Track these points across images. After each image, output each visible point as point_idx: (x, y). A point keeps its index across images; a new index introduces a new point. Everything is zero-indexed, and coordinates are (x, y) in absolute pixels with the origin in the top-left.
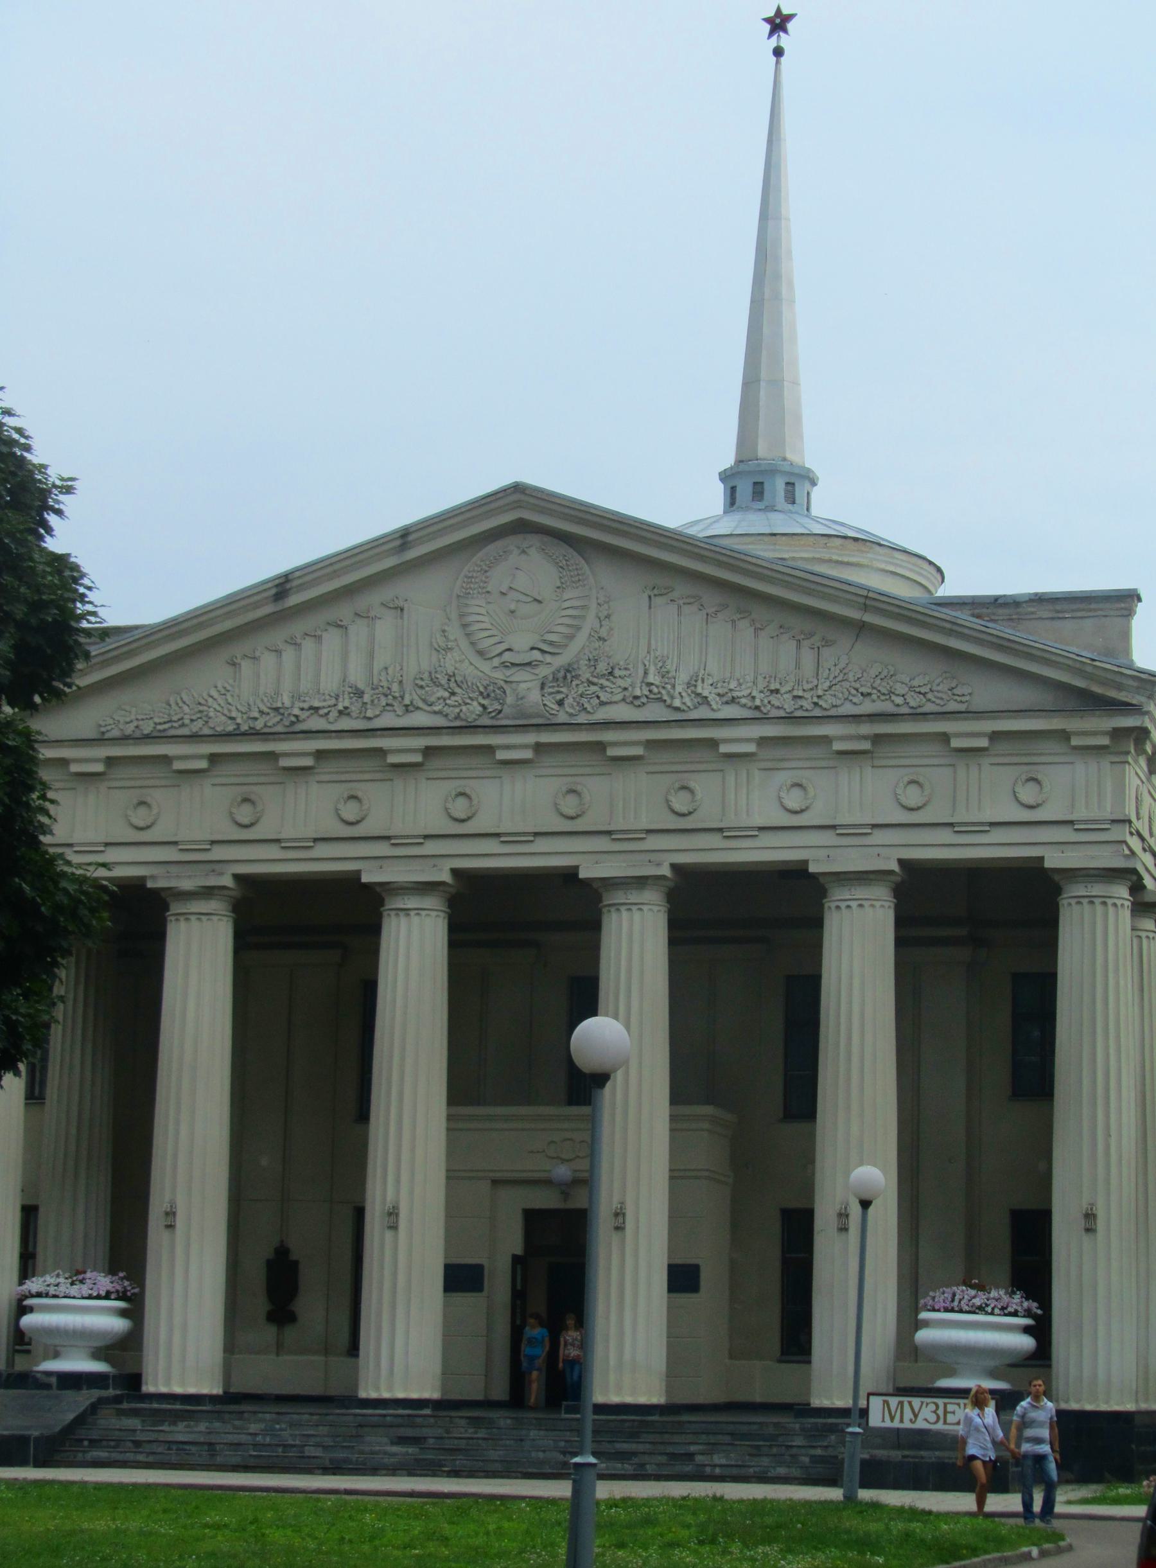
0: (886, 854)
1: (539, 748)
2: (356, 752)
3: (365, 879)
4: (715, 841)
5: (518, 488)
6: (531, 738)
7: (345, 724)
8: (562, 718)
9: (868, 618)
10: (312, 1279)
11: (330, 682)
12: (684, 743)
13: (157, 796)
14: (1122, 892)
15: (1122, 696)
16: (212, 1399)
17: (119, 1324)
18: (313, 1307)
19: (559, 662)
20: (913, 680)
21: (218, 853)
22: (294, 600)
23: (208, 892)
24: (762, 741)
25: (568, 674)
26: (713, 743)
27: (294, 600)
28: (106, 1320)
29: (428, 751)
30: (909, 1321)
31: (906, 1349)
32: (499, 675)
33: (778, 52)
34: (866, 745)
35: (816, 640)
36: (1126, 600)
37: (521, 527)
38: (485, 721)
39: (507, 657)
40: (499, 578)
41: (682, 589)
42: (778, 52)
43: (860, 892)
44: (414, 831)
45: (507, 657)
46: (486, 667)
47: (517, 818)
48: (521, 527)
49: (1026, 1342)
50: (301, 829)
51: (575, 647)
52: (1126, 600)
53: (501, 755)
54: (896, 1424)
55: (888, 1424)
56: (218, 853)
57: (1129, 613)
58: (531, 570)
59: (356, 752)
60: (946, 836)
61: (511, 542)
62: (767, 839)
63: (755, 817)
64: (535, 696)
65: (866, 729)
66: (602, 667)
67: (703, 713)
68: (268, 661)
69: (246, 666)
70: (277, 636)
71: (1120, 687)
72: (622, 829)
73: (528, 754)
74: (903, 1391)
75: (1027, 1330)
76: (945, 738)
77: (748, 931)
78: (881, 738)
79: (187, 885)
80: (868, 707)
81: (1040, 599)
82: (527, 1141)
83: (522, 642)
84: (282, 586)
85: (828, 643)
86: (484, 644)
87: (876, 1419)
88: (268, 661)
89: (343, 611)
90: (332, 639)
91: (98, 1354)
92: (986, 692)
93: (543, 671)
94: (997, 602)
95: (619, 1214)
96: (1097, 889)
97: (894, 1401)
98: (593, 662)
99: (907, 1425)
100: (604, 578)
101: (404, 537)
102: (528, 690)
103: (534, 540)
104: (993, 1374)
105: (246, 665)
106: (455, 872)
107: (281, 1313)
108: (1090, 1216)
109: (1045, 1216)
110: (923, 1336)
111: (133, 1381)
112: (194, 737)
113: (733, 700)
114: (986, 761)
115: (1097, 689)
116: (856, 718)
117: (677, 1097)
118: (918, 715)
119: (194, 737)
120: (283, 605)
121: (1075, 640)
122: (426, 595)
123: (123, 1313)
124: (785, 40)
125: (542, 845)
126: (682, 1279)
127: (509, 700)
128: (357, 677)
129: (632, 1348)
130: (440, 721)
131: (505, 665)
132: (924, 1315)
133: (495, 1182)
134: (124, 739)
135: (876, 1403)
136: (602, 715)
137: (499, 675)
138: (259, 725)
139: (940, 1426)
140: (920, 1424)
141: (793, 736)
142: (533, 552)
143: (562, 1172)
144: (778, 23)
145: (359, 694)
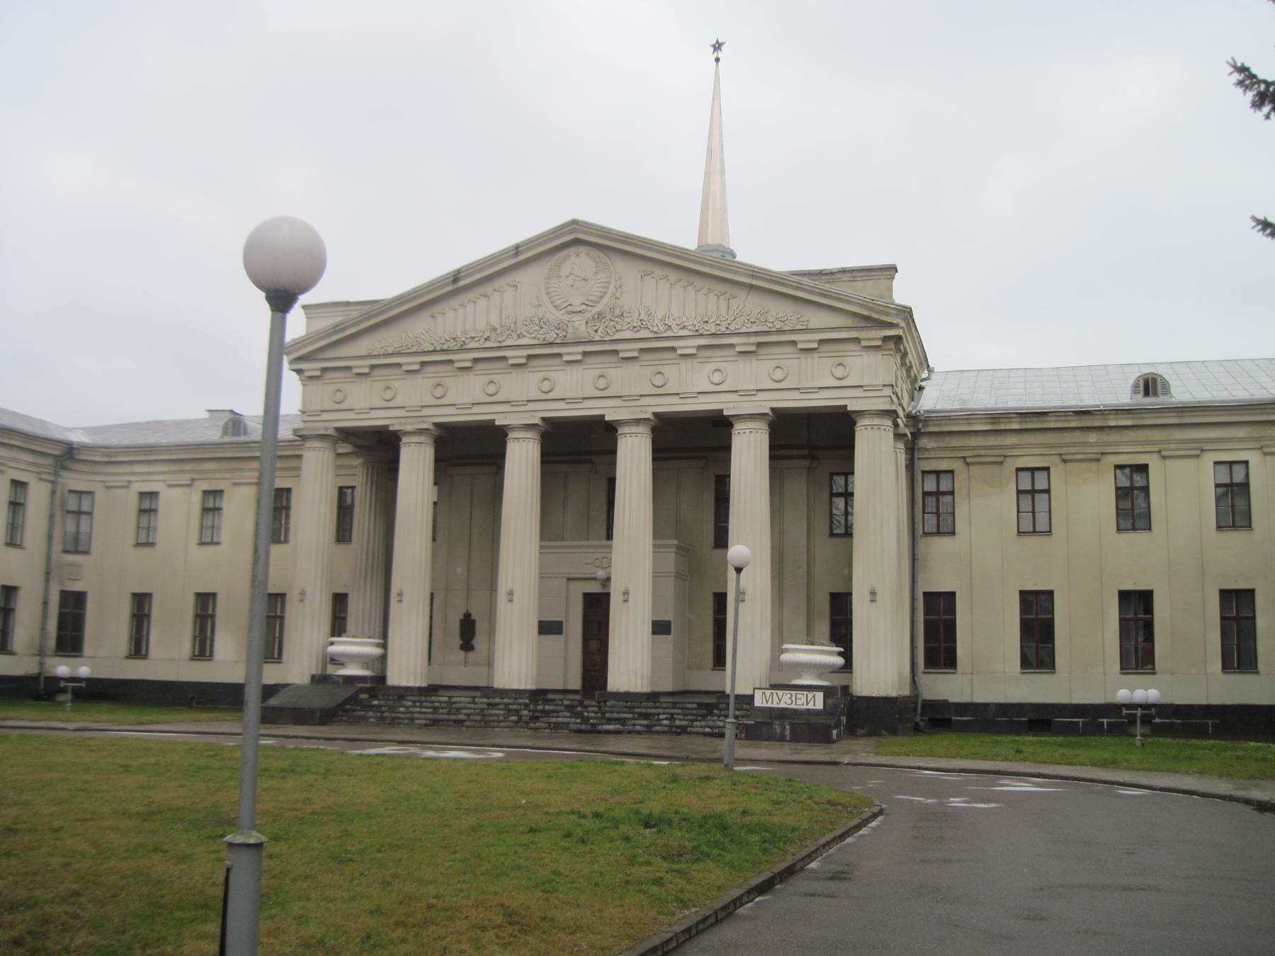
0: (764, 404)
1: (585, 354)
2: (491, 358)
3: (497, 423)
4: (675, 400)
5: (574, 222)
6: (581, 349)
7: (488, 344)
8: (597, 338)
9: (755, 282)
10: (480, 627)
11: (481, 325)
12: (658, 349)
13: (395, 384)
14: (888, 422)
15: (889, 319)
16: (420, 689)
17: (377, 651)
18: (479, 641)
19: (595, 310)
20: (778, 313)
21: (426, 412)
22: (462, 283)
23: (420, 432)
24: (700, 347)
25: (600, 314)
26: (673, 349)
27: (462, 283)
28: (369, 649)
29: (530, 357)
30: (777, 650)
31: (776, 664)
32: (566, 318)
33: (717, 60)
34: (753, 348)
35: (727, 296)
36: (892, 269)
37: (577, 242)
38: (558, 341)
39: (569, 308)
40: (565, 270)
41: (658, 271)
42: (717, 60)
43: (751, 425)
44: (520, 400)
45: (569, 308)
46: (558, 314)
47: (575, 391)
48: (577, 242)
49: (840, 661)
50: (465, 399)
51: (604, 302)
52: (892, 269)
53: (566, 358)
54: (769, 705)
55: (765, 705)
56: (426, 412)
57: (893, 278)
58: (580, 262)
59: (491, 358)
60: (795, 395)
61: (572, 251)
62: (702, 398)
63: (694, 388)
64: (583, 328)
65: (754, 339)
66: (617, 312)
67: (670, 334)
68: (450, 314)
69: (440, 318)
70: (454, 302)
71: (887, 314)
72: (628, 396)
73: (579, 357)
74: (774, 687)
75: (840, 654)
76: (794, 343)
77: (692, 445)
78: (762, 345)
79: (409, 428)
80: (754, 329)
81: (844, 271)
82: (577, 559)
83: (576, 301)
84: (456, 276)
85: (734, 297)
86: (558, 303)
87: (758, 702)
88: (450, 314)
89: (487, 289)
90: (482, 303)
91: (366, 665)
92: (818, 319)
93: (589, 315)
94: (821, 274)
95: (626, 593)
96: (876, 421)
97: (768, 692)
98: (612, 310)
99: (775, 705)
100: (620, 266)
101: (517, 249)
102: (579, 326)
103: (583, 250)
104: (820, 677)
105: (440, 318)
106: (543, 419)
107: (467, 646)
108: (873, 593)
109: (849, 595)
110: (785, 657)
111: (381, 679)
112: (415, 353)
113: (684, 327)
114: (816, 356)
115: (875, 316)
116: (748, 334)
117: (658, 533)
118: (780, 332)
119: (415, 353)
120: (458, 285)
121: (866, 290)
122: (530, 279)
123: (378, 645)
124: (720, 55)
125: (587, 404)
126: (660, 628)
127: (570, 330)
128: (495, 321)
129: (633, 664)
130: (536, 342)
131: (568, 313)
132: (785, 646)
133: (569, 579)
134: (378, 356)
135: (758, 694)
136: (617, 336)
137: (566, 318)
138: (445, 347)
139: (793, 706)
140: (782, 705)
141: (714, 344)
142: (583, 256)
143: (601, 574)
144: (717, 47)
145: (494, 329)
